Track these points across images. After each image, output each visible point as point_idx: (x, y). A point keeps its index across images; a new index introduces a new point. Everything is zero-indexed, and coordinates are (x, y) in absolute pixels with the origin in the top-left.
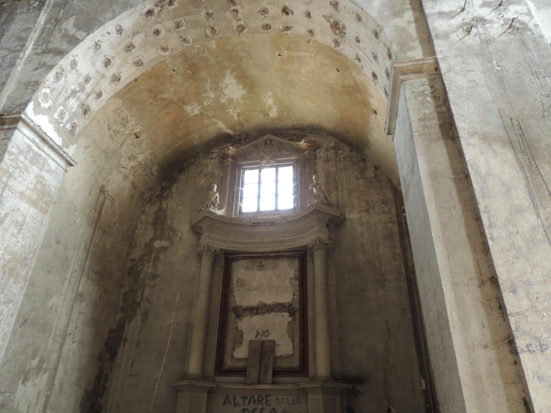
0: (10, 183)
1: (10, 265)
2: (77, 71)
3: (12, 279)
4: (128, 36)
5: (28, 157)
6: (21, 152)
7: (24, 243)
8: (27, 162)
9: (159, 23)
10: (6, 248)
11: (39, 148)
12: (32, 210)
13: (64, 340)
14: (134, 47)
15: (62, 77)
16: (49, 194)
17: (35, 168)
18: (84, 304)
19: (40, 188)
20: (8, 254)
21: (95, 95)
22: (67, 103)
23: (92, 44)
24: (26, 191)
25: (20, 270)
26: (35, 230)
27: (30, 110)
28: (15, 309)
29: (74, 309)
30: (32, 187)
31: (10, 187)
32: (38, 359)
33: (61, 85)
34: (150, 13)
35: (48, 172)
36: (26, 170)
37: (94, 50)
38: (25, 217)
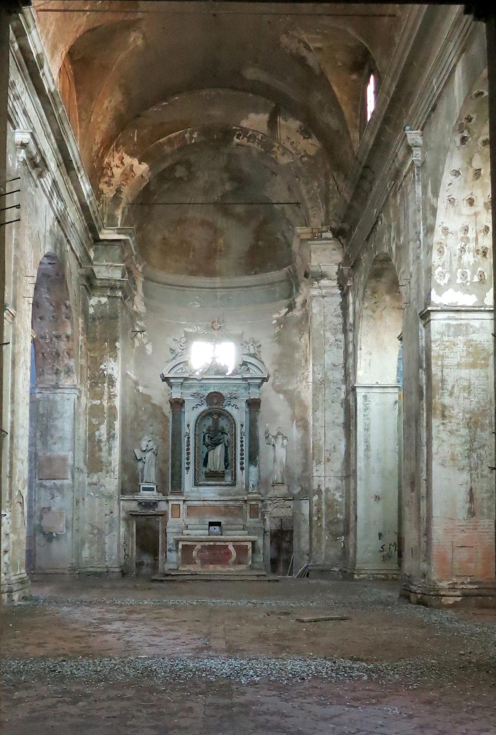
2: (451, 233)
3: (479, 430)
4: (467, 169)
5: (451, 334)
7: (476, 400)
9: (478, 138)
14: (480, 170)
15: (443, 248)
16: (483, 350)
19: (472, 351)
20: (467, 414)
21: (482, 234)
22: (462, 262)
23: (446, 201)
24: (461, 360)
25: (483, 421)
26: (483, 385)
27: (435, 298)
28: (491, 449)
31: (447, 366)
33: (447, 256)
34: (464, 140)
36: (454, 345)
37: (451, 206)
38: (469, 380)
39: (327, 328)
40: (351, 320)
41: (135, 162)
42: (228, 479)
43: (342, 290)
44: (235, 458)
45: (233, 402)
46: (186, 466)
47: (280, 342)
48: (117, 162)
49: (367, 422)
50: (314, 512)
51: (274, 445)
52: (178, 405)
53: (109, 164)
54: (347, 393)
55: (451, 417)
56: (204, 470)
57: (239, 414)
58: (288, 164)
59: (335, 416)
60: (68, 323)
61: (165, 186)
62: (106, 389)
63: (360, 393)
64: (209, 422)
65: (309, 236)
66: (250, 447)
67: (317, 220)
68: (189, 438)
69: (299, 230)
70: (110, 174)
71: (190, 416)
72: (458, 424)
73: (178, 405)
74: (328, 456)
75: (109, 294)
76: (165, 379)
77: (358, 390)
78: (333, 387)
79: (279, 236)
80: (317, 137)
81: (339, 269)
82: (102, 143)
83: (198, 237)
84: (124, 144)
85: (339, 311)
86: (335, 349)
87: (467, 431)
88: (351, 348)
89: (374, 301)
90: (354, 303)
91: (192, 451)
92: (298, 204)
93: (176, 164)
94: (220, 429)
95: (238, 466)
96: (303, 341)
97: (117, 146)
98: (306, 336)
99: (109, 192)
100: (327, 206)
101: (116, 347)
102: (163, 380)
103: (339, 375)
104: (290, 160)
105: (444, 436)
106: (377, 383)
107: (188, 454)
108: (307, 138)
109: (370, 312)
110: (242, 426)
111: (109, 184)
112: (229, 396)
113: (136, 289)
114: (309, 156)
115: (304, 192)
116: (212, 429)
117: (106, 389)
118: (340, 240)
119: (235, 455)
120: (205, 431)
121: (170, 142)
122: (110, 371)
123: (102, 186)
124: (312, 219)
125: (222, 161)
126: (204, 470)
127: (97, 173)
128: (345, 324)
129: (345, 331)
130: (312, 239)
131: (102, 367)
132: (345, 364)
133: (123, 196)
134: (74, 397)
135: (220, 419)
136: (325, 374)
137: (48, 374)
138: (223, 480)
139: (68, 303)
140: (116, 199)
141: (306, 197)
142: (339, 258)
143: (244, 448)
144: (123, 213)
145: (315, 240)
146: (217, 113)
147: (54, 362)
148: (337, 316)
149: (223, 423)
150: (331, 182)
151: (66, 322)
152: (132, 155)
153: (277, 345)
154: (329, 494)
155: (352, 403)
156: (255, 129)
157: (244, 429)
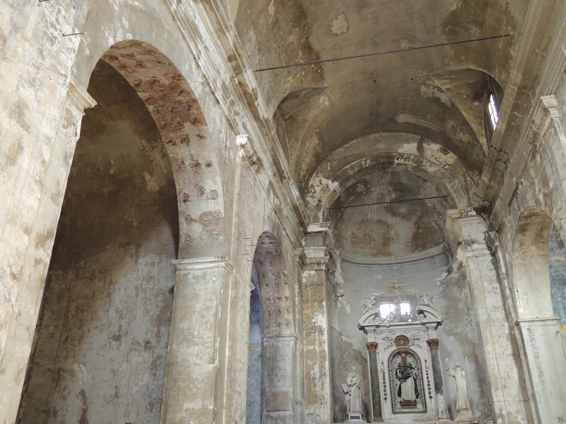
39: (484, 279)
40: (503, 270)
41: (330, 182)
42: (420, 407)
43: (491, 250)
44: (424, 389)
45: (416, 342)
46: (384, 397)
47: (445, 297)
48: (318, 183)
49: (536, 351)
52: (373, 347)
53: (312, 185)
54: (511, 329)
56: (399, 399)
57: (423, 352)
58: (435, 172)
59: (503, 348)
60: (286, 287)
61: (351, 199)
62: (317, 337)
63: (524, 327)
64: (399, 360)
65: (458, 216)
66: (435, 379)
67: (462, 203)
68: (384, 373)
69: (450, 212)
70: (313, 191)
71: (383, 355)
73: (373, 347)
74: (503, 383)
75: (316, 268)
76: (362, 328)
77: (522, 324)
79: (433, 224)
80: (453, 152)
81: (485, 236)
82: (307, 171)
83: (377, 232)
84: (321, 172)
85: (492, 267)
86: (493, 295)
88: (508, 292)
89: (523, 251)
90: (504, 257)
91: (387, 384)
93: (357, 183)
94: (408, 365)
95: (427, 396)
96: (463, 295)
97: (317, 173)
98: (466, 291)
99: (313, 202)
100: (468, 195)
101: (323, 305)
102: (360, 329)
103: (501, 315)
107: (385, 386)
108: (446, 154)
109: (520, 261)
110: (426, 361)
111: (313, 197)
112: (412, 338)
113: (336, 267)
114: (450, 165)
115: (449, 187)
116: (402, 365)
117: (317, 337)
118: (482, 216)
119: (423, 385)
120: (396, 367)
121: (352, 168)
122: (319, 324)
123: (308, 199)
124: (458, 204)
125: (388, 178)
126: (399, 399)
127: (304, 190)
128: (498, 275)
129: (500, 281)
131: (314, 320)
133: (323, 204)
134: (292, 343)
135: (407, 357)
136: (489, 315)
137: (274, 327)
138: (416, 408)
139: (285, 272)
140: (318, 206)
141: (451, 191)
143: (429, 379)
144: (323, 214)
145: (463, 218)
146: (382, 146)
147: (277, 317)
148: (491, 270)
149: (410, 360)
150: (468, 179)
151: (284, 287)
152: (328, 178)
153: (443, 300)
155: (518, 336)
156: (409, 153)
157: (428, 364)
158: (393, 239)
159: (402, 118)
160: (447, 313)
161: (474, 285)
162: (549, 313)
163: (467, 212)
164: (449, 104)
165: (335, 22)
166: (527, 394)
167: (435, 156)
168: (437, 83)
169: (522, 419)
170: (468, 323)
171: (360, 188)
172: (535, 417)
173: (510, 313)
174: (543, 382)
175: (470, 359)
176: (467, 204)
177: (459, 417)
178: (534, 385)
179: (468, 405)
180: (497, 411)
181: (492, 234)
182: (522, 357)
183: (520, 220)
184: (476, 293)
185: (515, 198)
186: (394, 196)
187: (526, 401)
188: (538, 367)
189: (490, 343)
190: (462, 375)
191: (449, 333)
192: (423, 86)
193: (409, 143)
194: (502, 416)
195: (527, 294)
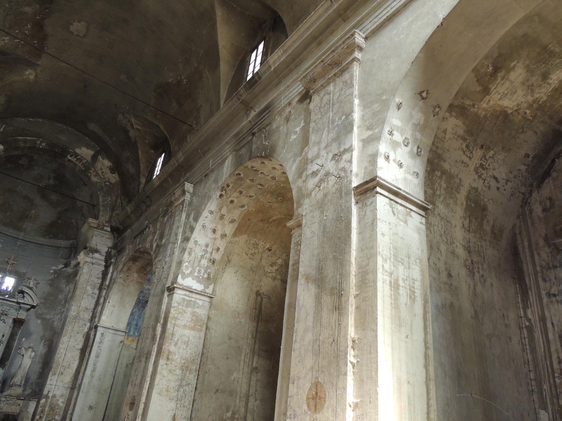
0: (177, 323)
1: (186, 365)
3: (188, 373)
6: (179, 304)
8: (184, 308)
10: (181, 357)
11: (189, 297)
12: (192, 333)
13: (248, 400)
17: (189, 309)
18: (259, 374)
29: (252, 378)
30: (190, 320)
32: (231, 412)
35: (198, 308)
39: (89, 284)
40: (107, 283)
47: (51, 285)
49: (99, 352)
50: (38, 412)
51: (23, 355)
54: (90, 329)
55: (172, 360)
58: (97, 182)
59: (76, 343)
63: (100, 330)
65: (96, 226)
67: (104, 217)
69: (90, 220)
72: (176, 366)
74: (62, 370)
77: (99, 328)
78: (81, 322)
79: (73, 221)
81: (108, 250)
85: (101, 276)
87: (181, 372)
88: (102, 300)
90: (113, 273)
92: (94, 206)
98: (71, 286)
103: (88, 316)
104: (98, 181)
105: (165, 373)
106: (113, 327)
109: (122, 281)
114: (110, 183)
115: (101, 200)
121: (25, 141)
124: (101, 217)
128: (102, 284)
130: (97, 228)
132: (94, 309)
136: (78, 313)
141: (101, 204)
142: (110, 244)
146: (63, 138)
148: (98, 278)
150: (119, 201)
153: (49, 287)
154: (54, 399)
155: (92, 337)
158: (31, 217)
159: (92, 127)
160: (45, 299)
161: (79, 286)
162: (123, 326)
163: (105, 226)
164: (133, 140)
165: (76, 24)
166: (76, 383)
167: (103, 171)
168: (133, 120)
169: (62, 402)
170: (60, 313)
171: (24, 161)
172: (73, 402)
173: (95, 317)
174: (92, 376)
175: (46, 343)
176: (107, 220)
177: (9, 392)
178: (85, 377)
179: (23, 382)
180: (45, 392)
181: (113, 252)
182: (87, 354)
183: (135, 252)
184: (78, 292)
185: (140, 236)
186: (52, 182)
187: (72, 389)
188: (95, 365)
189: (68, 335)
190: (30, 356)
191: (39, 316)
192: (121, 115)
193: (88, 149)
194: (47, 397)
195: (114, 307)
